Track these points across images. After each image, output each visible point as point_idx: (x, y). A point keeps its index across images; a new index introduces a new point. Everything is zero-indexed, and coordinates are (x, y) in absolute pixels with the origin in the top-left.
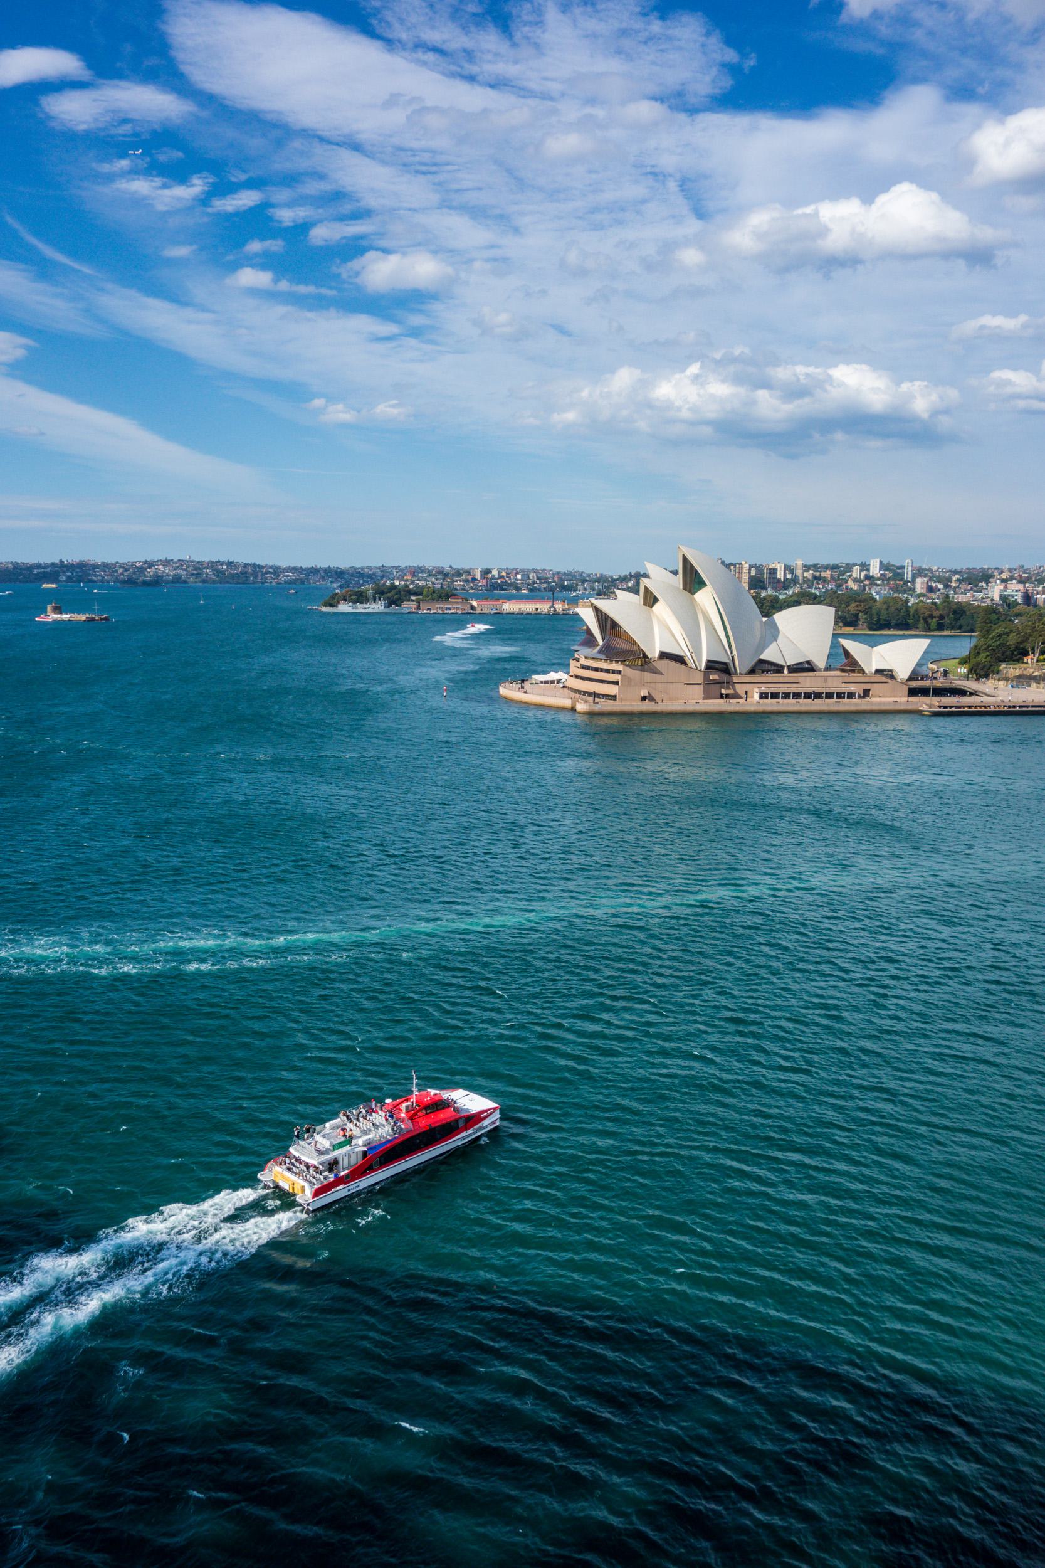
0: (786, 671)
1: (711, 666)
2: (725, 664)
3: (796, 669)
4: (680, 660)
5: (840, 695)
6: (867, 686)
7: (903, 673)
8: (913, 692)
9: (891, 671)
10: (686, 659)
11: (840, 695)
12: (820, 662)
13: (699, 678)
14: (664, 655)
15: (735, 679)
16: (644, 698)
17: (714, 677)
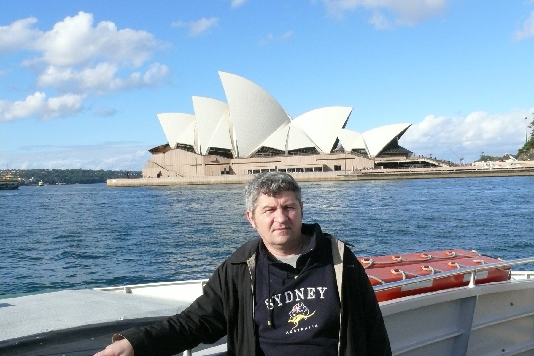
0: (286, 153)
1: (213, 151)
2: (229, 150)
4: (189, 148)
5: (309, 170)
6: (338, 163)
7: (374, 150)
8: (378, 165)
9: (365, 149)
10: (195, 147)
11: (309, 170)
12: (325, 147)
13: (200, 160)
14: (180, 146)
15: (232, 161)
16: (159, 175)
17: (213, 158)
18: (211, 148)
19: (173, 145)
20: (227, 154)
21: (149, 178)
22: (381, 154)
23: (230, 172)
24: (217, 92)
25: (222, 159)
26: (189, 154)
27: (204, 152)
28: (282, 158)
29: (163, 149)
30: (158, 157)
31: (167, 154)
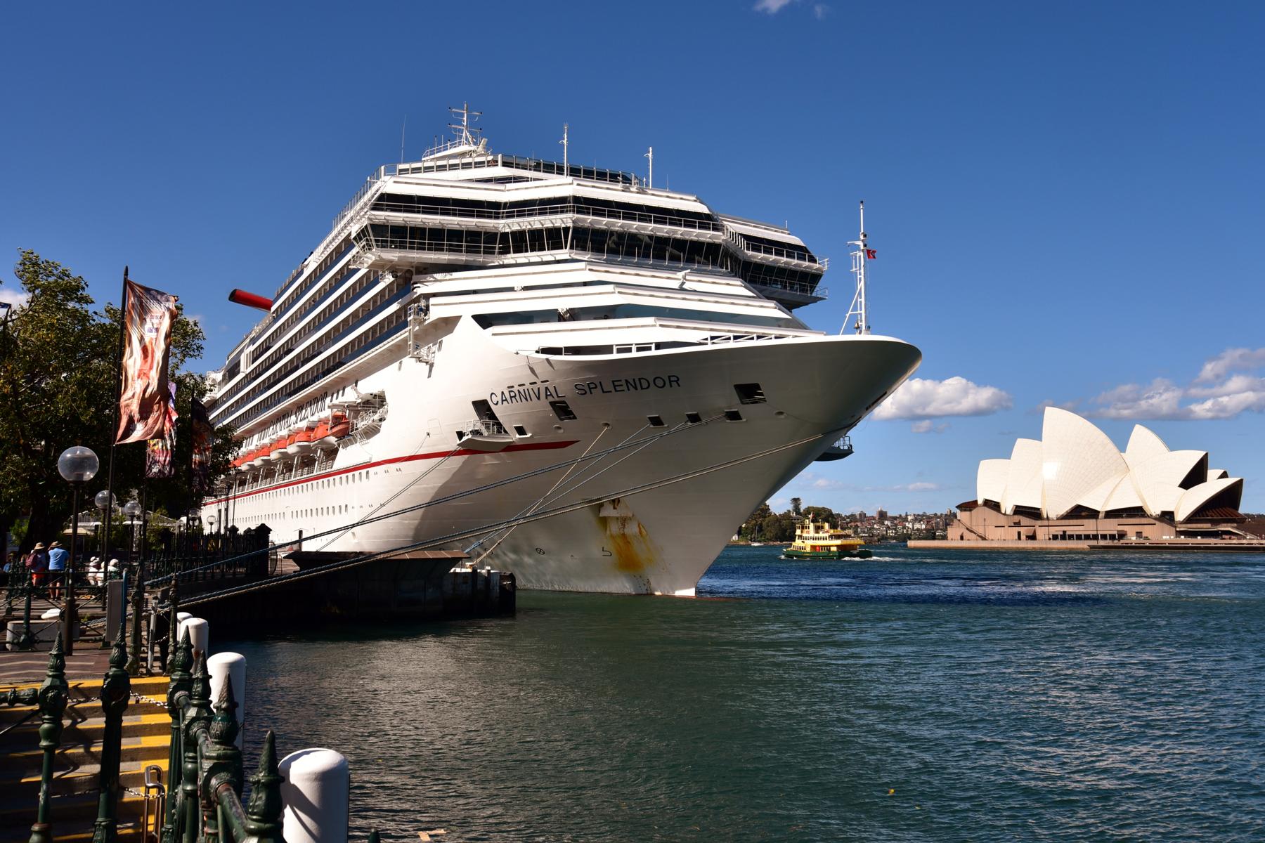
0: (1101, 515)
3: (1111, 514)
14: (987, 503)
15: (1039, 523)
18: (1017, 507)
19: (980, 502)
20: (1034, 513)
21: (954, 539)
22: (1189, 520)
23: (1032, 537)
24: (1037, 435)
25: (1025, 521)
26: (994, 513)
27: (1009, 511)
28: (1085, 522)
29: (969, 506)
30: (963, 516)
31: (974, 511)
